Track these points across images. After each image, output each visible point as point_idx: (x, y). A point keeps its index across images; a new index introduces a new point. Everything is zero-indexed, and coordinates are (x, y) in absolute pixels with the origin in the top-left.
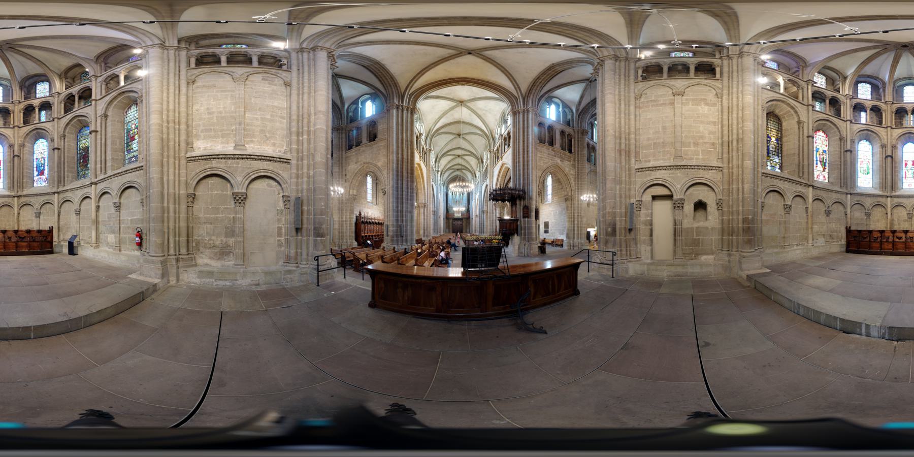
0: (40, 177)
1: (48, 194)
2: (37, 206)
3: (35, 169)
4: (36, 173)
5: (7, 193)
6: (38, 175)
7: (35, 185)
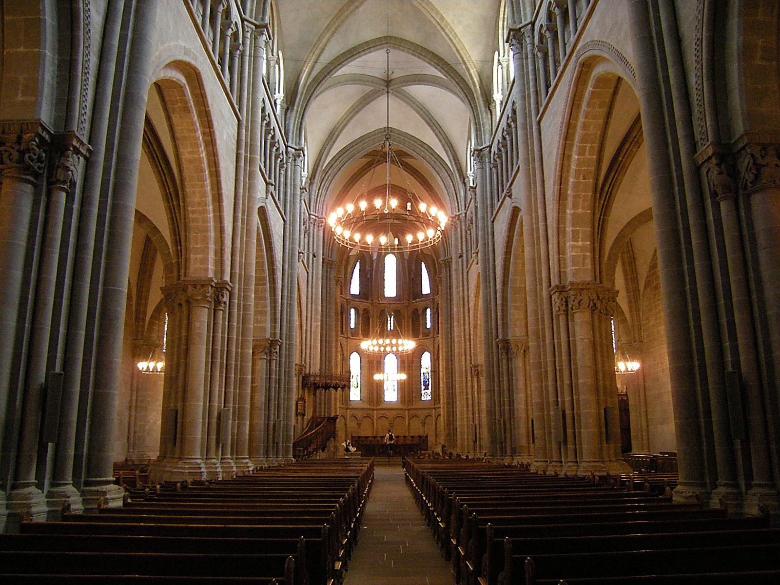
0: (426, 391)
1: (429, 408)
2: (423, 417)
3: (422, 383)
4: (423, 387)
5: (401, 407)
6: (424, 390)
7: (423, 399)
